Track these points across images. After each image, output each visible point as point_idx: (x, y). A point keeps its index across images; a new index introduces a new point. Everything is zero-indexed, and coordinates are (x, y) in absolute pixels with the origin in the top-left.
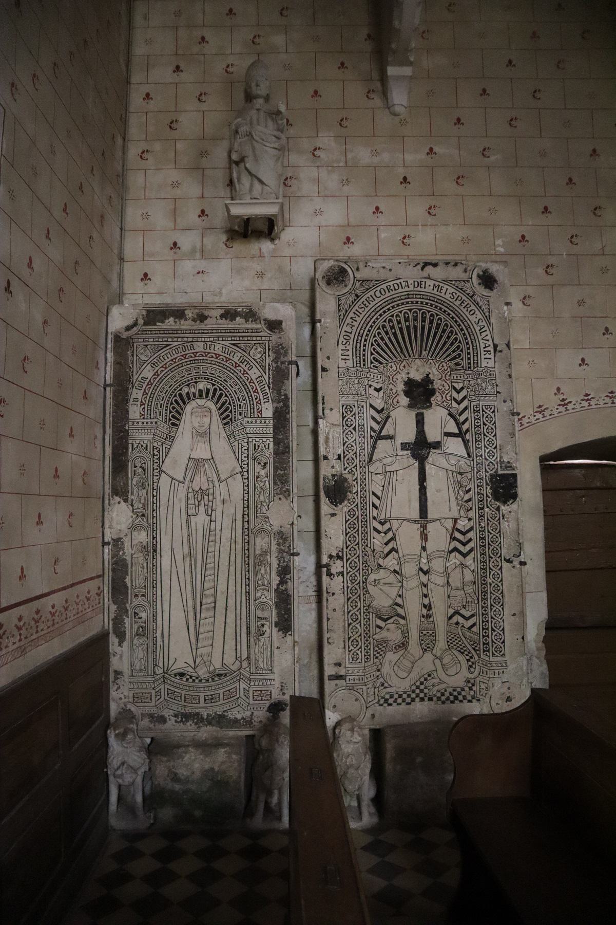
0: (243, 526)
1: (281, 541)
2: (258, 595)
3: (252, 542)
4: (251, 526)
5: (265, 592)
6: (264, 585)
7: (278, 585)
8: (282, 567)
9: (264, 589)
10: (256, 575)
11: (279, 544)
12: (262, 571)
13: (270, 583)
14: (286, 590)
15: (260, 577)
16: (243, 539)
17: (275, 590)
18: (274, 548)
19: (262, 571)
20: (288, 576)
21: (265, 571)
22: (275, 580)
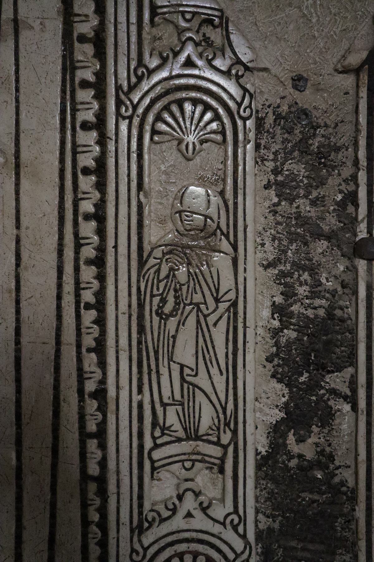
0: (69, 66)
1: (297, 168)
2: (161, 490)
3: (120, 169)
4: (120, 72)
5: (203, 479)
6: (192, 434)
7: (277, 432)
8: (304, 325)
9: (193, 460)
10: (146, 362)
11: (284, 188)
12: (185, 353)
13: (230, 421)
14: (325, 459)
15: (169, 385)
16: (68, 150)
17: (263, 462)
18: (255, 207)
19: (185, 353)
20: (337, 381)
21: (204, 349)
22: (262, 401)
